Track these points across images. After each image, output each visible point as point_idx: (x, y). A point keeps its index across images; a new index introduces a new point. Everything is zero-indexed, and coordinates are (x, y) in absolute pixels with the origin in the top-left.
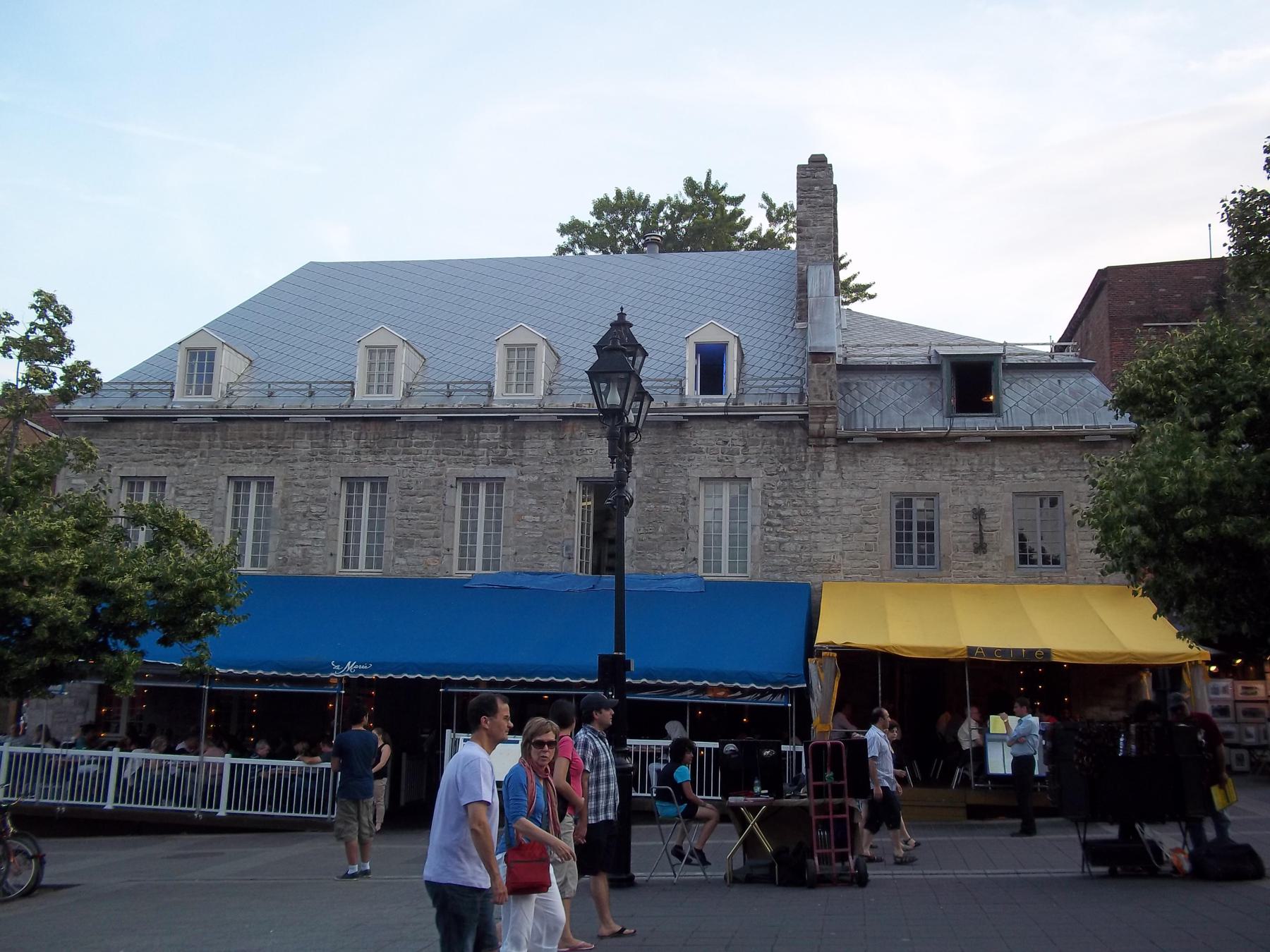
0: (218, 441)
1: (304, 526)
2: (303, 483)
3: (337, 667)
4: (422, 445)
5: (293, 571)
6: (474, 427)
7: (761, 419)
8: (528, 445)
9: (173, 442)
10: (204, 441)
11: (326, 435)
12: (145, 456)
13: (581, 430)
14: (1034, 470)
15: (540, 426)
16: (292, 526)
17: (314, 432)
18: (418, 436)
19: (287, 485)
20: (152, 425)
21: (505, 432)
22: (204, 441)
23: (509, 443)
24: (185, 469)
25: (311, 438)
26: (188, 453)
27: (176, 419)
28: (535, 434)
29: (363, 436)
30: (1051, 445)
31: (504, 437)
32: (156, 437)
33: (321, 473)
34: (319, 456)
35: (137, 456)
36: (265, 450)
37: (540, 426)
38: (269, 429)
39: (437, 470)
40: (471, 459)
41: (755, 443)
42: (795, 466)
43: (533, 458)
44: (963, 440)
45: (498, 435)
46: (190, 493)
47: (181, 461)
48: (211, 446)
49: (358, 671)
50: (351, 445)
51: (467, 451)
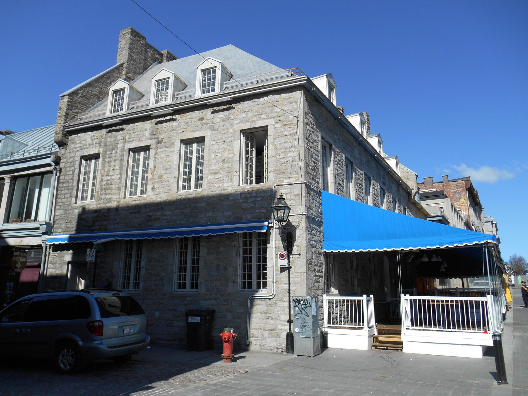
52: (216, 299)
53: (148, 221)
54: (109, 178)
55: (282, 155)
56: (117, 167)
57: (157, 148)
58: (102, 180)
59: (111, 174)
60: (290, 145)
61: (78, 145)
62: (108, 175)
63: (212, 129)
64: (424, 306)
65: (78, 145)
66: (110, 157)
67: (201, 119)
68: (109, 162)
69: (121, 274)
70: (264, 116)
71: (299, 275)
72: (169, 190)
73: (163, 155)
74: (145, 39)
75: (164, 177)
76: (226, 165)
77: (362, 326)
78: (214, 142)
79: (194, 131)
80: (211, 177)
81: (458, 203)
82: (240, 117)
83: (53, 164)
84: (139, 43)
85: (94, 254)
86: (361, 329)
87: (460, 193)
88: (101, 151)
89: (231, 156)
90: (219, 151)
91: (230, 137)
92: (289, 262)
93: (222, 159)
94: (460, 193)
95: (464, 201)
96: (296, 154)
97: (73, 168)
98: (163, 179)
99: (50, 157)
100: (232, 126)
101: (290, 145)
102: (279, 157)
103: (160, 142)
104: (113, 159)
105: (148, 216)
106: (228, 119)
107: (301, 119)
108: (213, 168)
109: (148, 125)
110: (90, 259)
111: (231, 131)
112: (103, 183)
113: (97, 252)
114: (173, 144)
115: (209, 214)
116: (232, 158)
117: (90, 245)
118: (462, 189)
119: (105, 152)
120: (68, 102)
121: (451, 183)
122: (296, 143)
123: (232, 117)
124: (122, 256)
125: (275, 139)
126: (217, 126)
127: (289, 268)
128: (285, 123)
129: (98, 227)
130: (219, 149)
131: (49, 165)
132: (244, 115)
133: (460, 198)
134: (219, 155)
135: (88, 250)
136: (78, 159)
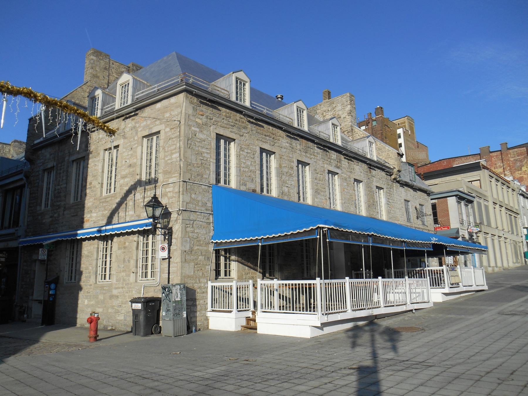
1: (287, 178)
2: (286, 158)
5: (286, 198)
9: (237, 122)
12: (225, 126)
16: (284, 177)
19: (281, 158)
24: (243, 137)
26: (243, 131)
32: (230, 117)
33: (291, 156)
35: (223, 125)
36: (271, 139)
39: (322, 165)
40: (330, 164)
43: (344, 168)
46: (246, 151)
50: (298, 147)
51: (329, 160)
52: (122, 288)
54: (59, 187)
55: (169, 158)
56: (64, 178)
58: (55, 190)
59: (61, 183)
60: (174, 147)
61: (42, 161)
62: (59, 185)
63: (124, 137)
64: (302, 288)
65: (42, 161)
66: (61, 169)
68: (60, 173)
69: (67, 268)
70: (158, 122)
71: (176, 265)
72: (95, 195)
73: (93, 164)
75: (93, 183)
76: (131, 170)
77: (345, 310)
78: (125, 150)
80: (122, 181)
81: (520, 172)
82: (142, 125)
83: (24, 178)
84: (102, 61)
85: (46, 253)
86: (231, 312)
87: (521, 161)
88: (55, 165)
89: (135, 161)
90: (128, 157)
91: (135, 144)
94: (521, 161)
95: (526, 169)
96: (178, 155)
97: (38, 181)
98: (92, 185)
99: (22, 173)
100: (137, 133)
101: (174, 147)
102: (166, 159)
104: (62, 171)
106: (134, 127)
107: (183, 122)
108: (124, 173)
110: (43, 257)
111: (136, 138)
112: (56, 192)
113: (49, 251)
114: (99, 154)
116: (136, 163)
117: (41, 246)
118: (523, 156)
121: (511, 151)
122: (178, 145)
123: (137, 125)
124: (68, 253)
126: (127, 136)
127: (169, 258)
128: (172, 127)
129: (52, 230)
130: (128, 155)
131: (22, 179)
132: (145, 123)
133: (522, 166)
134: (128, 161)
135: (40, 249)
136: (40, 173)
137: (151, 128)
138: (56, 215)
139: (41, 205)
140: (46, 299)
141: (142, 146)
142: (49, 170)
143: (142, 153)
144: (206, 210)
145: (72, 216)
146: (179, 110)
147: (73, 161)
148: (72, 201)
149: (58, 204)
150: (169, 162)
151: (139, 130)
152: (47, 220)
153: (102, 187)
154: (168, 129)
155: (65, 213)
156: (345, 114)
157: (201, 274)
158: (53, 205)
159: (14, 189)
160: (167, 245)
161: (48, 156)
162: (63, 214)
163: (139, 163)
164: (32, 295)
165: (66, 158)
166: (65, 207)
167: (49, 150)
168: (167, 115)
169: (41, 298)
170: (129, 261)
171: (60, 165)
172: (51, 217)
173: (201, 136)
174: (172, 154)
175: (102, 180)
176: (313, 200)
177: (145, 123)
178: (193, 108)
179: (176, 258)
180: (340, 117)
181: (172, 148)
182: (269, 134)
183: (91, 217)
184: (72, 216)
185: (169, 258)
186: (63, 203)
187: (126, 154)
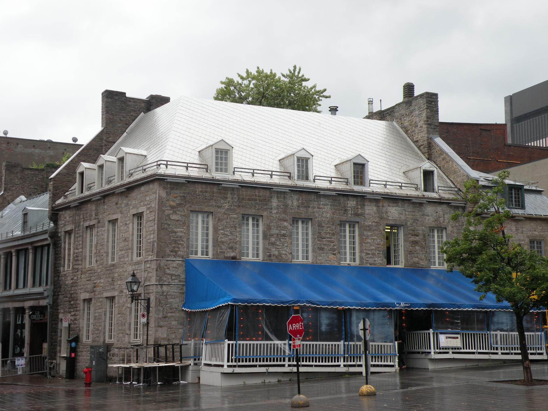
0: (236, 196)
3: (398, 305)
4: (325, 205)
5: (275, 261)
6: (345, 198)
7: (452, 204)
8: (367, 208)
10: (229, 195)
11: (284, 197)
13: (386, 204)
14: (535, 231)
15: (371, 200)
17: (279, 195)
18: (323, 201)
20: (204, 186)
21: (357, 202)
22: (229, 195)
23: (359, 207)
25: (278, 198)
26: (222, 201)
27: (220, 184)
28: (369, 204)
29: (300, 199)
30: (539, 222)
31: (357, 204)
34: (282, 207)
36: (258, 201)
37: (371, 200)
38: (259, 193)
41: (447, 214)
42: (461, 224)
44: (517, 218)
45: (355, 202)
47: (219, 205)
48: (232, 198)
49: (405, 307)
53: (95, 287)
56: (81, 243)
57: (98, 228)
61: (63, 222)
63: (121, 213)
65: (63, 222)
67: (117, 204)
74: (125, 93)
76: (126, 244)
79: (113, 214)
83: (49, 238)
92: (148, 319)
93: (124, 239)
100: (129, 211)
103: (99, 222)
105: (95, 283)
109: (91, 207)
114: (105, 224)
115: (119, 282)
116: (128, 238)
119: (75, 228)
120: (53, 184)
123: (129, 203)
125: (146, 223)
127: (148, 323)
131: (46, 239)
137: (138, 208)
138: (75, 278)
139: (64, 267)
140: (69, 356)
141: (133, 223)
142: (69, 233)
143: (133, 229)
144: (180, 281)
145: (88, 280)
146: (154, 196)
147: (87, 227)
148: (87, 266)
149: (77, 267)
150: (149, 241)
151: (131, 208)
152: (69, 282)
153: (107, 256)
154: (148, 212)
155: (83, 276)
156: (422, 122)
157: (174, 336)
158: (73, 268)
159: (42, 247)
160: (146, 313)
161: (68, 218)
162: (81, 278)
163: (131, 239)
164: (60, 352)
165: (82, 224)
166: (82, 271)
167: (68, 212)
168: (148, 199)
169: (65, 355)
170: (125, 324)
171: (77, 229)
172: (72, 279)
173: (174, 217)
174: (150, 234)
175: (108, 249)
176: (315, 257)
177: (134, 202)
178: (167, 192)
179: (152, 325)
180: (416, 126)
181: (151, 229)
182: (254, 197)
183: (100, 283)
184: (88, 280)
185: (148, 323)
186: (80, 267)
187: (122, 228)
